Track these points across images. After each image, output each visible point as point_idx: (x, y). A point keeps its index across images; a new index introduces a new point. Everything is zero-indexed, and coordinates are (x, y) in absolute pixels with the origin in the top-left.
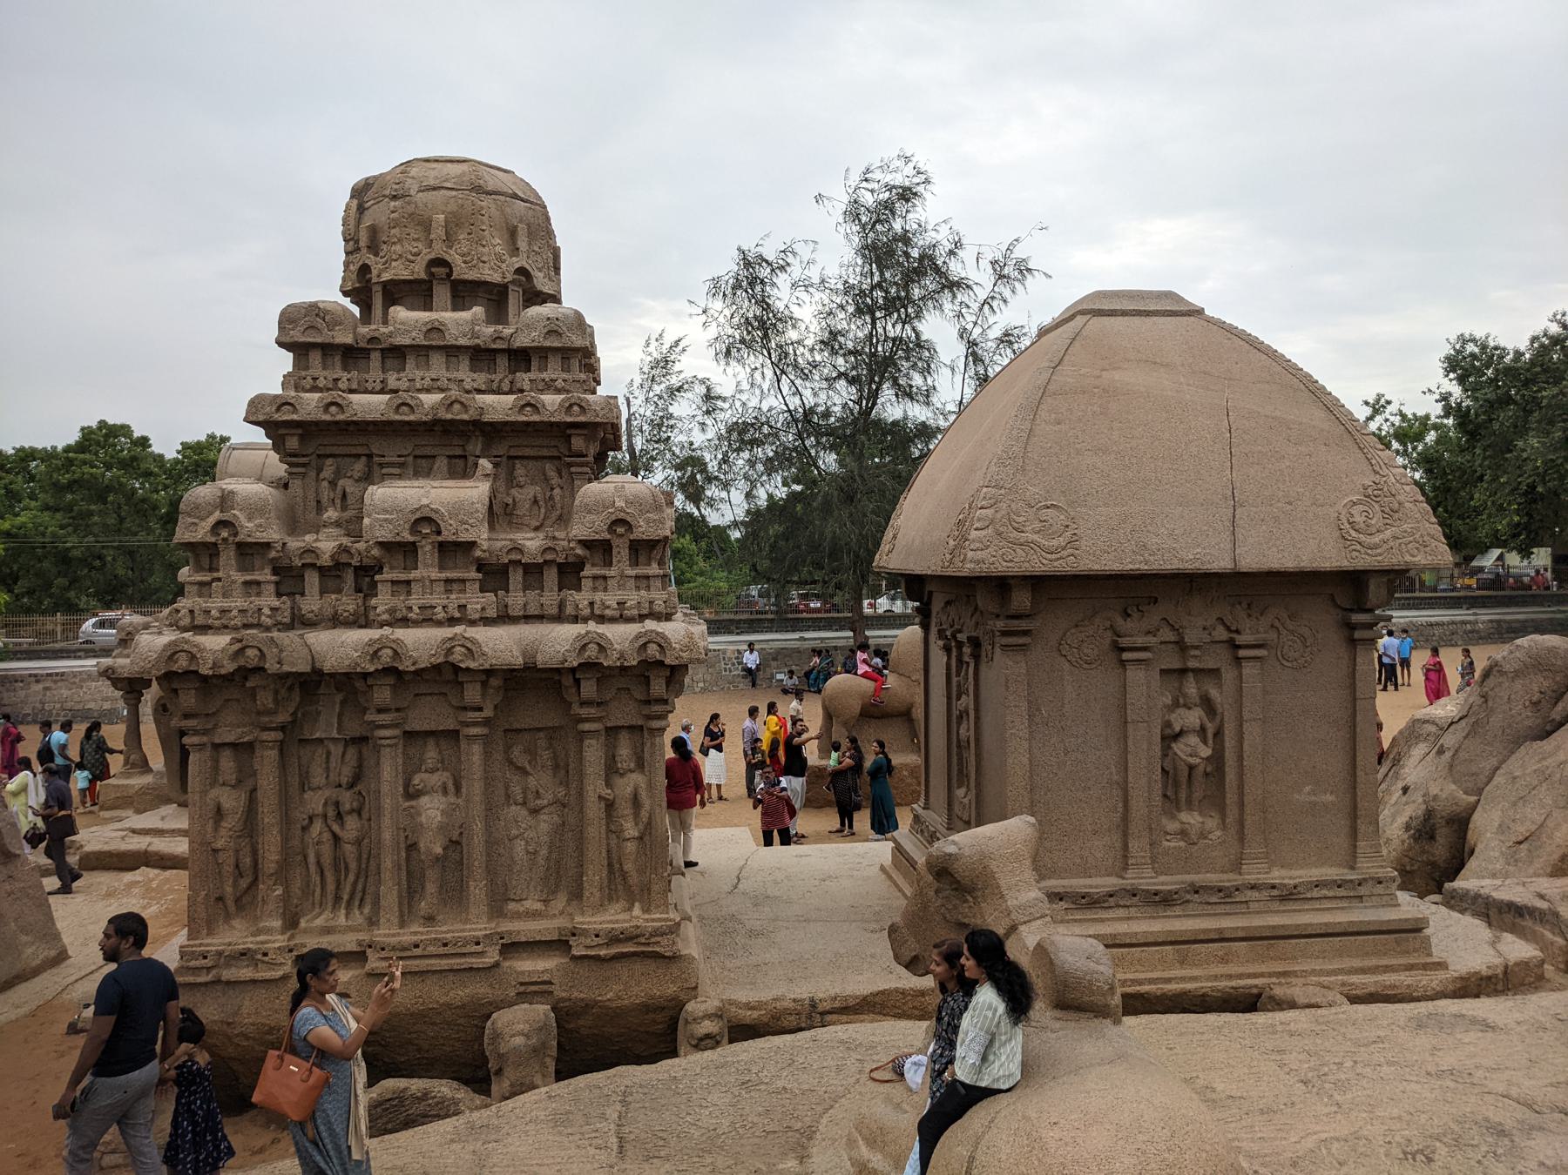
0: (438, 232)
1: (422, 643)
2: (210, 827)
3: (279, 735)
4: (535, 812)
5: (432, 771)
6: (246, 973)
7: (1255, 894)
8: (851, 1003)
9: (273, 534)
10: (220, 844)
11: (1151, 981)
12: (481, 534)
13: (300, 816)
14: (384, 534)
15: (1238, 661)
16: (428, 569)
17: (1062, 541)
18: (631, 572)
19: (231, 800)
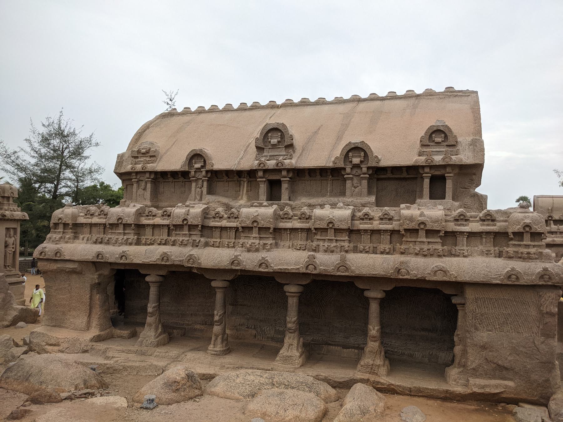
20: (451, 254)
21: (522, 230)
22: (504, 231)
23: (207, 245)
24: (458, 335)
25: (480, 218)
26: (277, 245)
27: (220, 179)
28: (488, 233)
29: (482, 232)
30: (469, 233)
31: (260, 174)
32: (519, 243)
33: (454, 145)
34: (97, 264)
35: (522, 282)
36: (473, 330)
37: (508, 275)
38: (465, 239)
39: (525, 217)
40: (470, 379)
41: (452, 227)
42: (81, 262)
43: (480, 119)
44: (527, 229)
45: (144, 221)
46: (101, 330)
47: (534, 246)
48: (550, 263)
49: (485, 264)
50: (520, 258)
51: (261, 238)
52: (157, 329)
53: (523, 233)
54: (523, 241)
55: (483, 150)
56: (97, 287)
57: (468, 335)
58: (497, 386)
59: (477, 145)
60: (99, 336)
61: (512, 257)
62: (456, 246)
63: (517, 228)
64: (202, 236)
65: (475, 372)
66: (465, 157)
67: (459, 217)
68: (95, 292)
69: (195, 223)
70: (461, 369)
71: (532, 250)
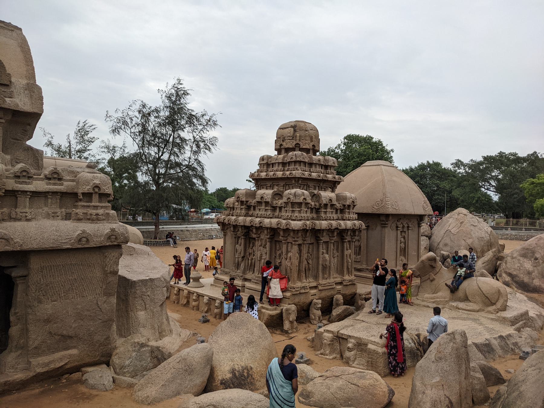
6: (303, 291)
15: (408, 229)
20: (11, 219)
21: (91, 191)
22: (71, 192)
24: (16, 313)
25: (46, 176)
28: (55, 193)
29: (48, 192)
30: (33, 192)
32: (88, 204)
33: (8, 85)
35: (92, 245)
36: (36, 304)
37: (79, 238)
38: (28, 199)
39: (94, 177)
40: (31, 360)
41: (11, 184)
43: (32, 61)
44: (97, 190)
47: (102, 207)
48: (116, 223)
49: (54, 228)
50: (89, 219)
53: (92, 193)
54: (91, 202)
55: (41, 98)
57: (30, 311)
58: (61, 359)
59: (34, 92)
61: (81, 219)
62: (16, 208)
63: (87, 189)
65: (38, 351)
66: (21, 102)
67: (21, 172)
70: (19, 352)
71: (101, 211)
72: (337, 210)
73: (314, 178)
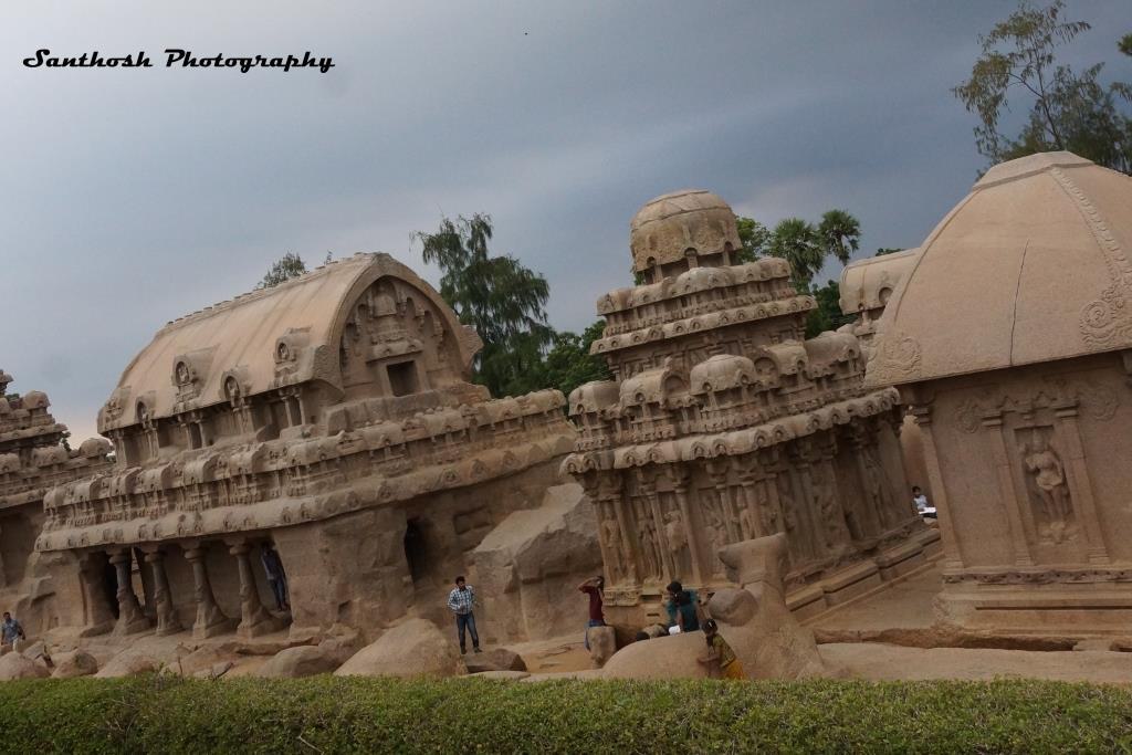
0: (648, 245)
1: (642, 452)
2: (605, 537)
3: (619, 496)
4: (717, 528)
5: (674, 510)
7: (1098, 578)
8: (877, 635)
9: (595, 409)
10: (610, 545)
11: (1020, 631)
12: (659, 398)
13: (638, 532)
14: (629, 403)
16: (646, 417)
17: (909, 362)
18: (717, 408)
19: (610, 524)
23: (135, 516)
26: (172, 508)
27: (166, 426)
31: (179, 419)
34: (75, 551)
42: (63, 551)
45: (102, 496)
46: (96, 623)
51: (160, 503)
52: (128, 617)
56: (84, 573)
58: (308, 633)
60: (92, 630)
64: (134, 505)
68: (85, 582)
69: (124, 492)
72: (764, 394)
73: (629, 345)
